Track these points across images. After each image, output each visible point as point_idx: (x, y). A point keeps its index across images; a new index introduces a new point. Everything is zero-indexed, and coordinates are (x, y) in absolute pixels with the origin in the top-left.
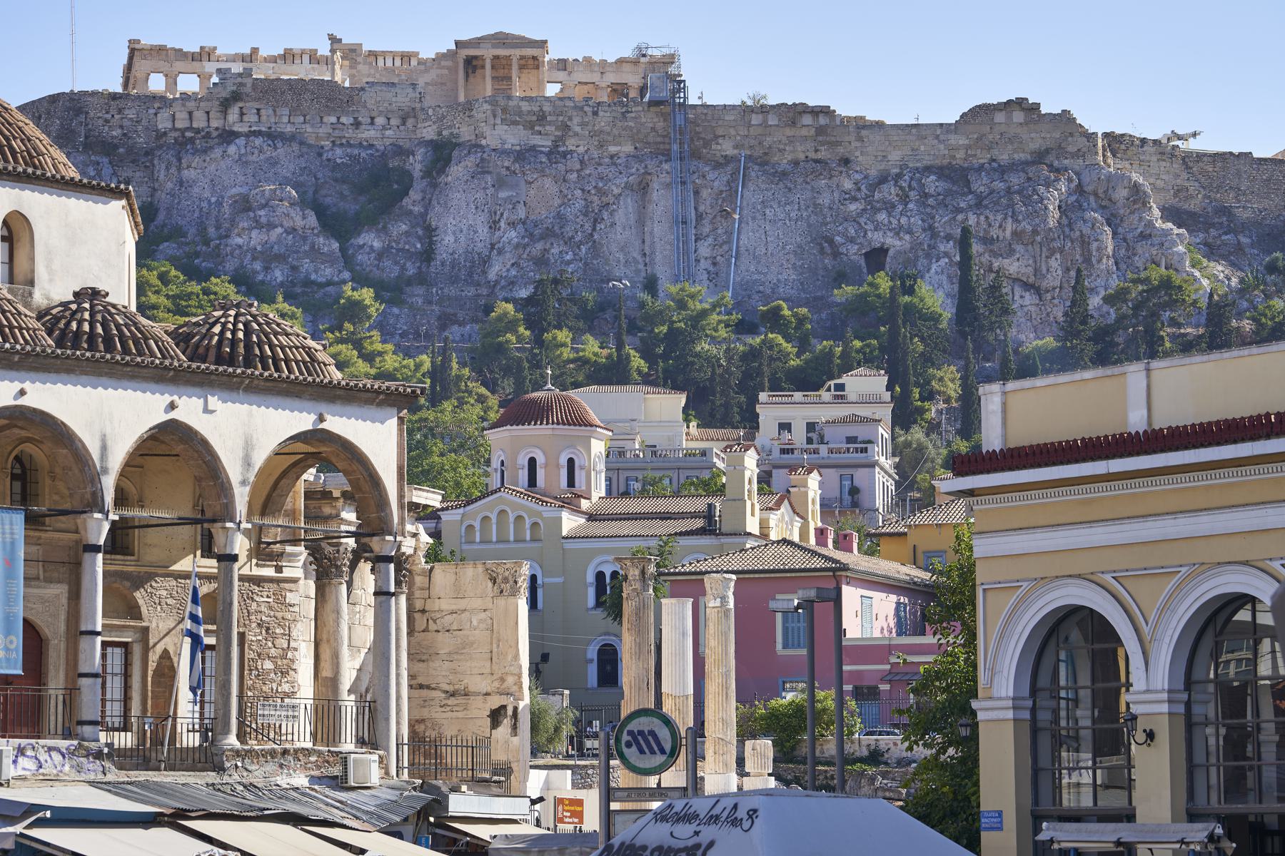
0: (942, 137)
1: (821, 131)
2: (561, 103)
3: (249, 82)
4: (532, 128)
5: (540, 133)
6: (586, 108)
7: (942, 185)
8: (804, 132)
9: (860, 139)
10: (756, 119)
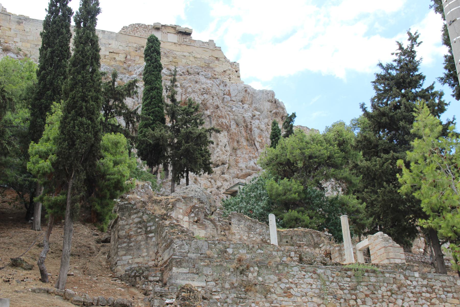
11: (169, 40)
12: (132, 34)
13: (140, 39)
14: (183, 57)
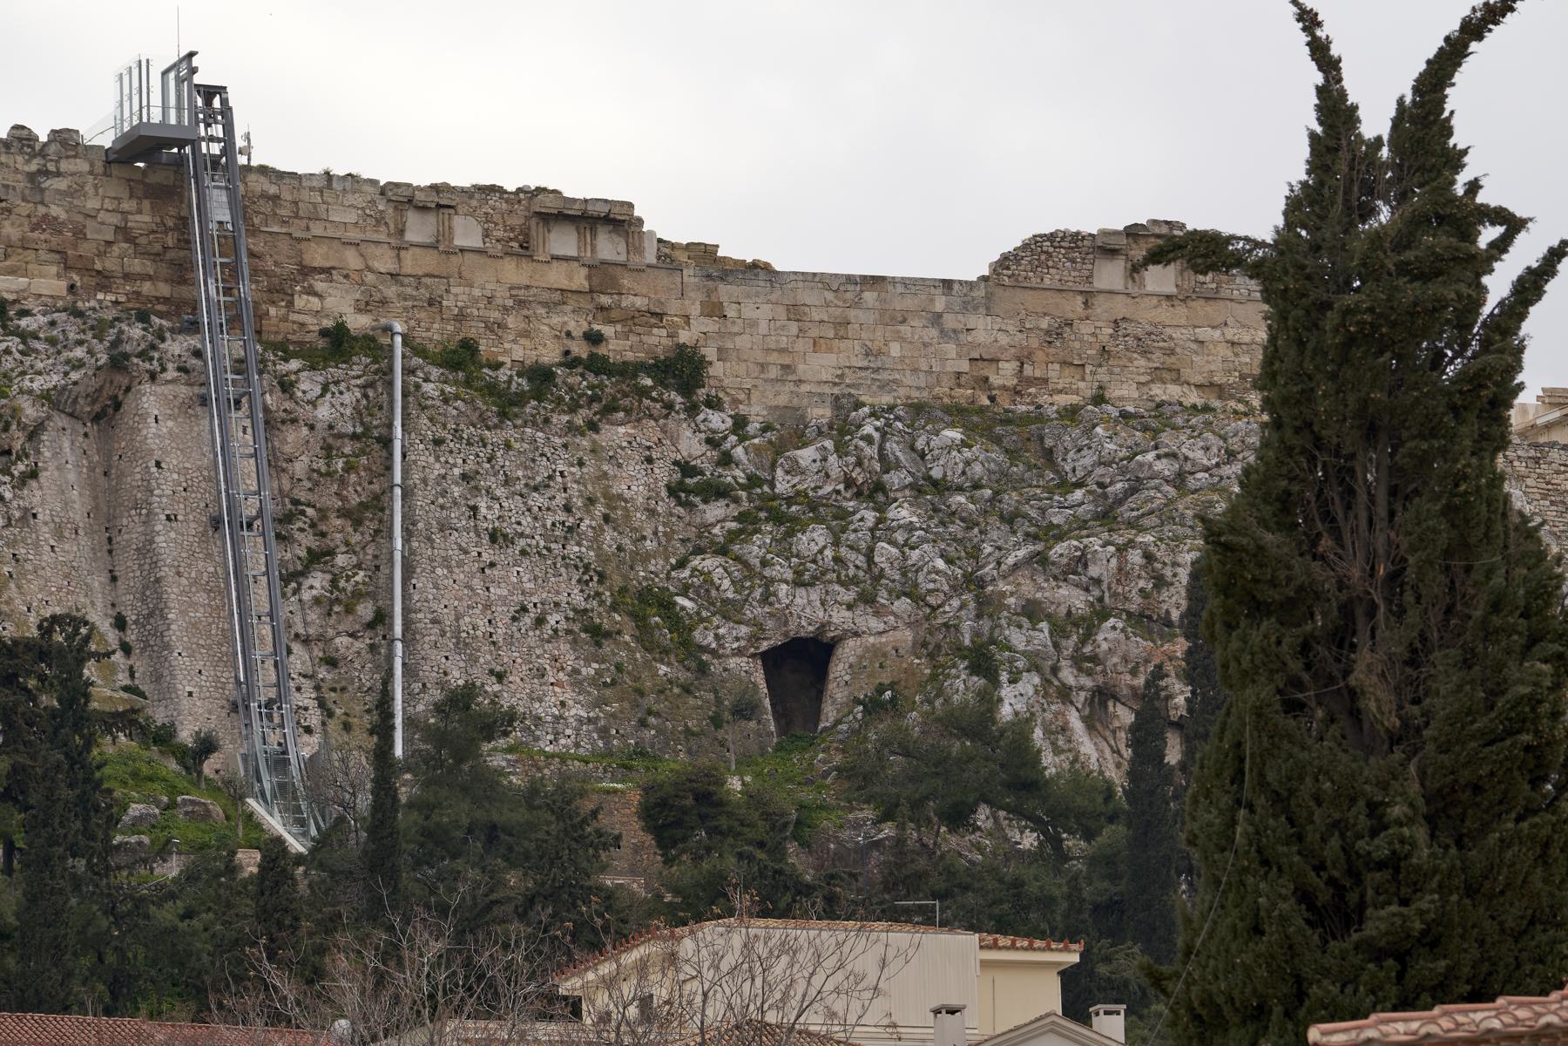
0: (950, 321)
1: (603, 276)
7: (983, 459)
8: (557, 276)
9: (714, 310)
10: (419, 229)
11: (1150, 288)
12: (1034, 281)
13: (1057, 298)
14: (1194, 346)
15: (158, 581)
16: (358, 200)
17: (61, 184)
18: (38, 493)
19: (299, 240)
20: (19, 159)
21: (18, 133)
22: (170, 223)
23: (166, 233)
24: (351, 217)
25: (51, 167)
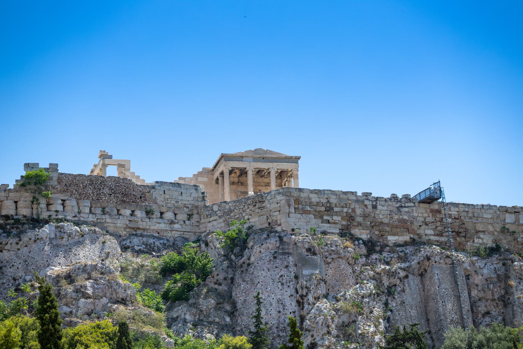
2: (345, 197)
3: (55, 176)
4: (321, 217)
5: (328, 222)
6: (366, 202)
15: (441, 320)
16: (491, 211)
17: (406, 209)
18: (405, 297)
19: (475, 223)
20: (394, 203)
21: (393, 196)
22: (438, 220)
23: (436, 222)
24: (489, 216)
25: (403, 205)
